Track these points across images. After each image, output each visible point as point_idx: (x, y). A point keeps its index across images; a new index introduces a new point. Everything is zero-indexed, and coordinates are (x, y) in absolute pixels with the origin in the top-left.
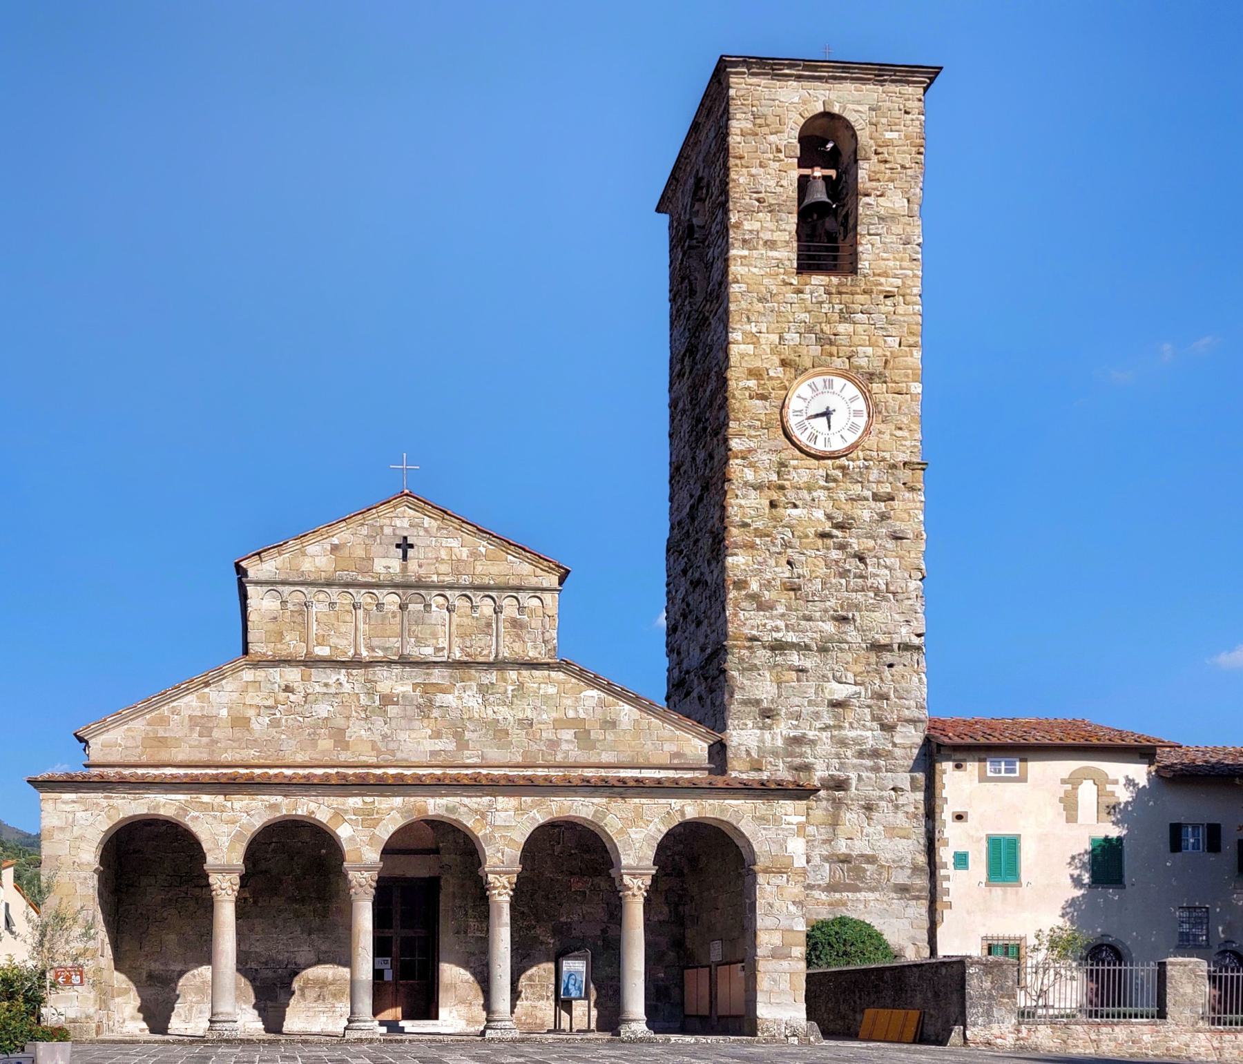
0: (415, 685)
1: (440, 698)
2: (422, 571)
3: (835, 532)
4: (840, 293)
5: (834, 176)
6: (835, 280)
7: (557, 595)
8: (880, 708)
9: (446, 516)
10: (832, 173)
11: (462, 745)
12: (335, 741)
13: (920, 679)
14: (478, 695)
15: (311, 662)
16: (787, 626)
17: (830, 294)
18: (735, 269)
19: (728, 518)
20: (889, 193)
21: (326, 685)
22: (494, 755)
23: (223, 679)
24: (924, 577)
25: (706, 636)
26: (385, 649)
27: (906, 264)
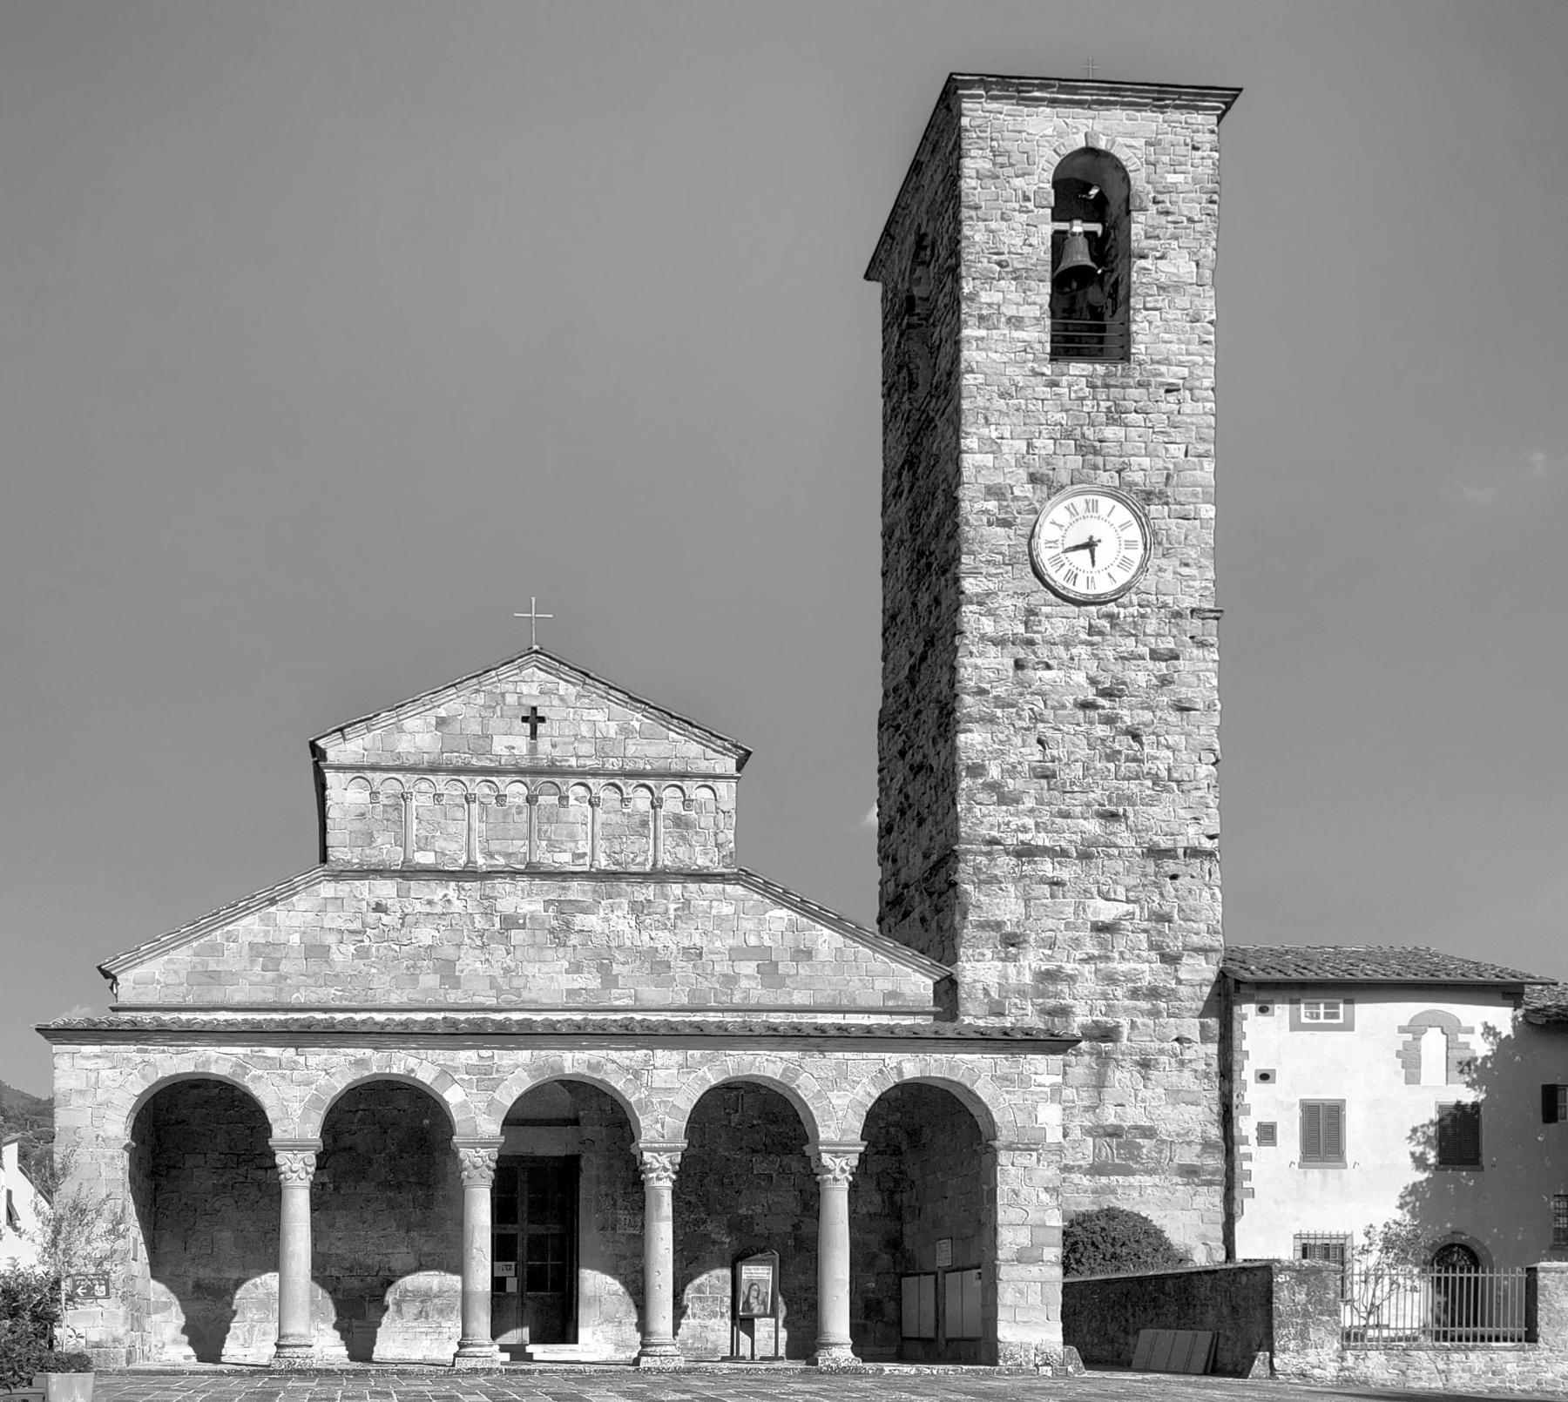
9: (588, 681)
12: (441, 976)
15: (410, 872)
21: (430, 902)
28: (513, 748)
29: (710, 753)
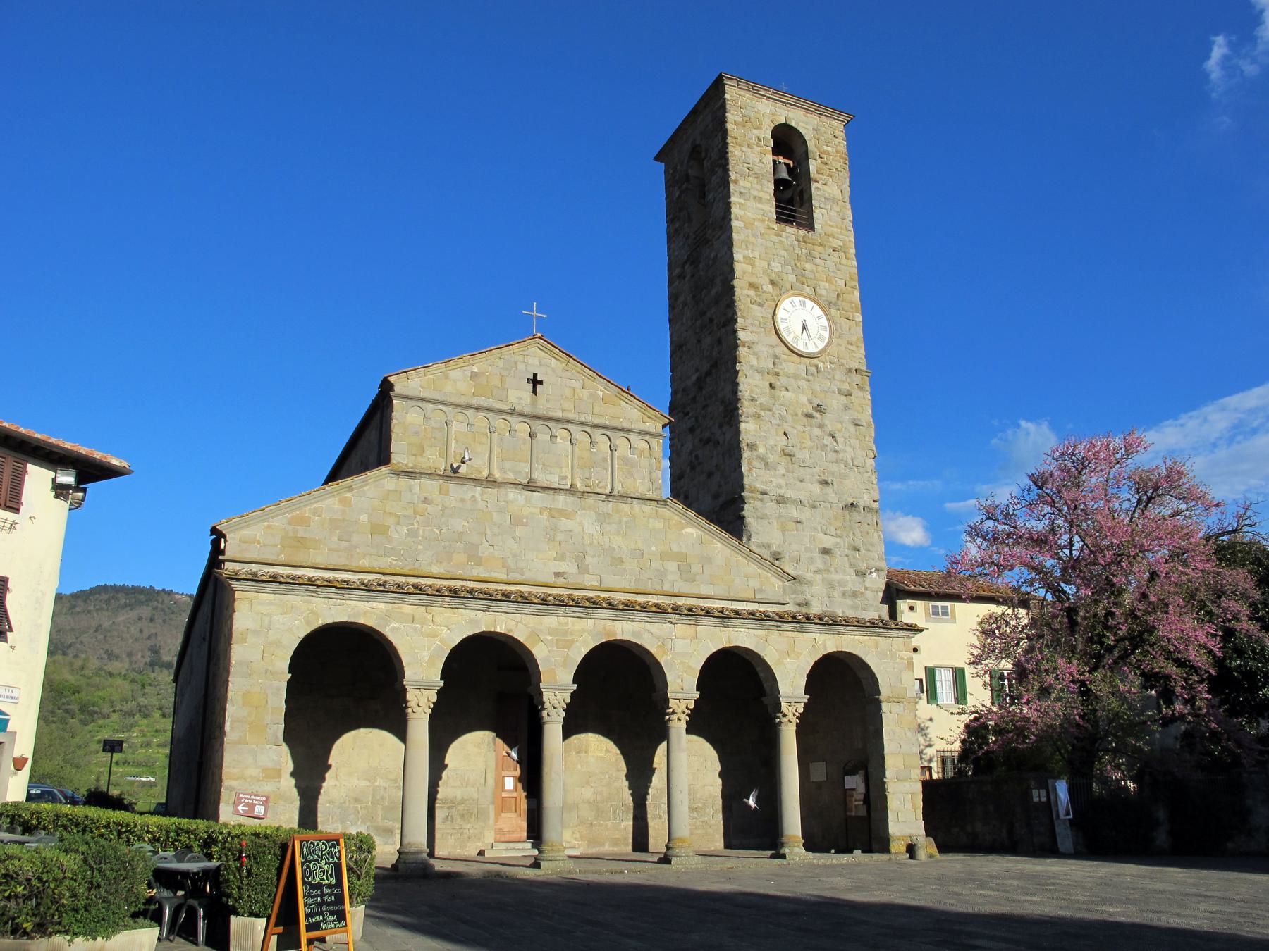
0: (542, 510)
1: (565, 524)
2: (548, 405)
3: (815, 414)
4: (805, 242)
5: (792, 166)
6: (801, 232)
7: (661, 441)
8: (855, 557)
10: (791, 163)
11: (583, 569)
13: (879, 536)
14: (596, 523)
16: (787, 484)
17: (799, 241)
18: (735, 210)
19: (740, 392)
20: (829, 184)
21: (462, 500)
22: (611, 581)
23: (365, 485)
24: (875, 457)
25: (720, 486)
27: (844, 232)
28: (521, 399)
29: (646, 418)
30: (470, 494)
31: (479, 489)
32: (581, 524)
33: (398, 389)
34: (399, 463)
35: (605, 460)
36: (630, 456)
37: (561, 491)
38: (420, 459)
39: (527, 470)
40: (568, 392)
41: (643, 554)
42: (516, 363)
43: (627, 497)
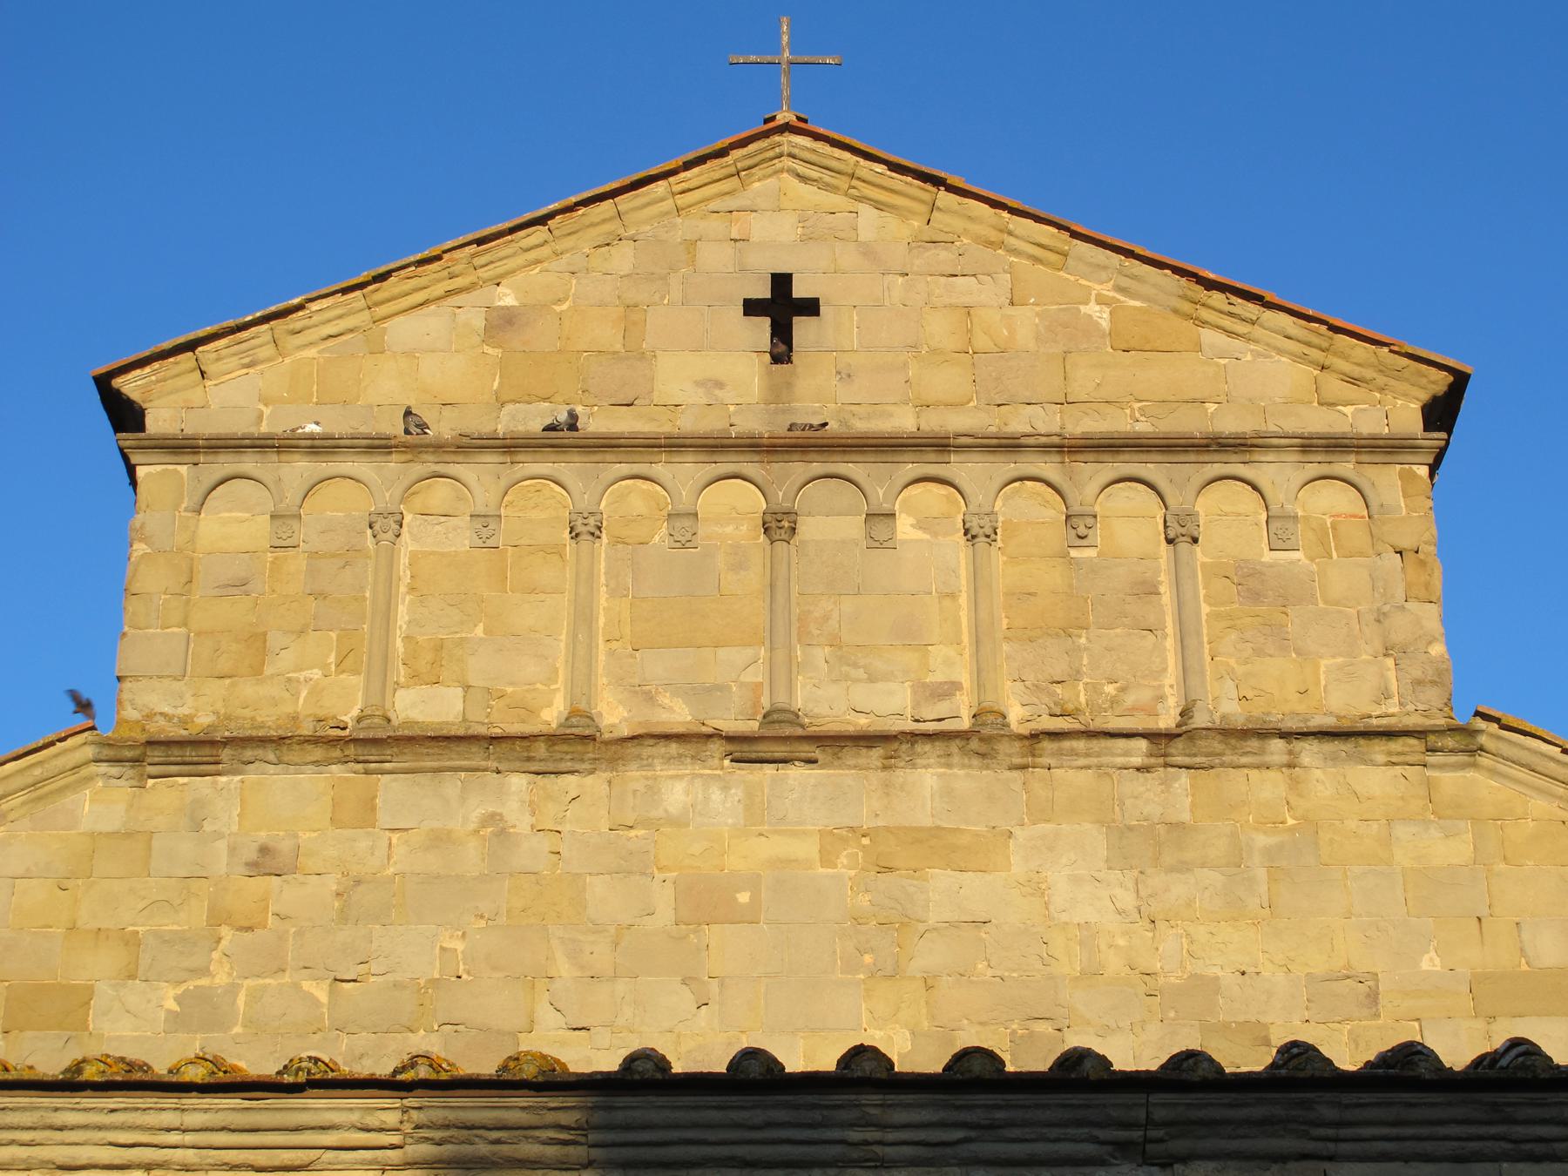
0: (830, 843)
21: (440, 840)
26: (701, 693)
28: (720, 385)
29: (1334, 386)
30: (477, 809)
31: (518, 782)
32: (1037, 888)
33: (158, 421)
34: (150, 716)
35: (1150, 590)
36: (1268, 557)
37: (922, 747)
38: (249, 689)
39: (756, 675)
40: (940, 330)
41: (1373, 997)
42: (691, 245)
43: (1263, 734)
